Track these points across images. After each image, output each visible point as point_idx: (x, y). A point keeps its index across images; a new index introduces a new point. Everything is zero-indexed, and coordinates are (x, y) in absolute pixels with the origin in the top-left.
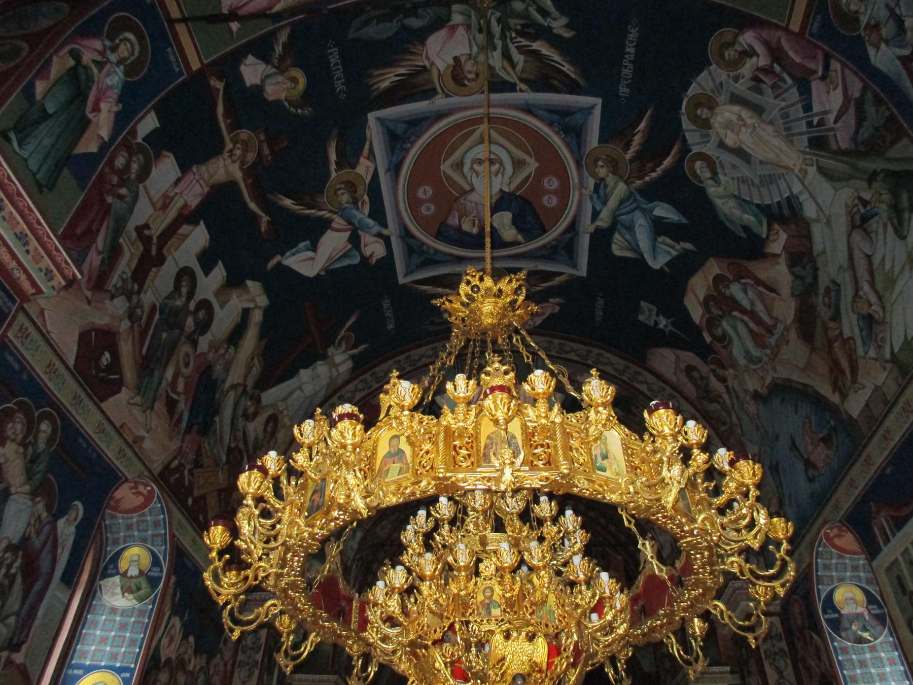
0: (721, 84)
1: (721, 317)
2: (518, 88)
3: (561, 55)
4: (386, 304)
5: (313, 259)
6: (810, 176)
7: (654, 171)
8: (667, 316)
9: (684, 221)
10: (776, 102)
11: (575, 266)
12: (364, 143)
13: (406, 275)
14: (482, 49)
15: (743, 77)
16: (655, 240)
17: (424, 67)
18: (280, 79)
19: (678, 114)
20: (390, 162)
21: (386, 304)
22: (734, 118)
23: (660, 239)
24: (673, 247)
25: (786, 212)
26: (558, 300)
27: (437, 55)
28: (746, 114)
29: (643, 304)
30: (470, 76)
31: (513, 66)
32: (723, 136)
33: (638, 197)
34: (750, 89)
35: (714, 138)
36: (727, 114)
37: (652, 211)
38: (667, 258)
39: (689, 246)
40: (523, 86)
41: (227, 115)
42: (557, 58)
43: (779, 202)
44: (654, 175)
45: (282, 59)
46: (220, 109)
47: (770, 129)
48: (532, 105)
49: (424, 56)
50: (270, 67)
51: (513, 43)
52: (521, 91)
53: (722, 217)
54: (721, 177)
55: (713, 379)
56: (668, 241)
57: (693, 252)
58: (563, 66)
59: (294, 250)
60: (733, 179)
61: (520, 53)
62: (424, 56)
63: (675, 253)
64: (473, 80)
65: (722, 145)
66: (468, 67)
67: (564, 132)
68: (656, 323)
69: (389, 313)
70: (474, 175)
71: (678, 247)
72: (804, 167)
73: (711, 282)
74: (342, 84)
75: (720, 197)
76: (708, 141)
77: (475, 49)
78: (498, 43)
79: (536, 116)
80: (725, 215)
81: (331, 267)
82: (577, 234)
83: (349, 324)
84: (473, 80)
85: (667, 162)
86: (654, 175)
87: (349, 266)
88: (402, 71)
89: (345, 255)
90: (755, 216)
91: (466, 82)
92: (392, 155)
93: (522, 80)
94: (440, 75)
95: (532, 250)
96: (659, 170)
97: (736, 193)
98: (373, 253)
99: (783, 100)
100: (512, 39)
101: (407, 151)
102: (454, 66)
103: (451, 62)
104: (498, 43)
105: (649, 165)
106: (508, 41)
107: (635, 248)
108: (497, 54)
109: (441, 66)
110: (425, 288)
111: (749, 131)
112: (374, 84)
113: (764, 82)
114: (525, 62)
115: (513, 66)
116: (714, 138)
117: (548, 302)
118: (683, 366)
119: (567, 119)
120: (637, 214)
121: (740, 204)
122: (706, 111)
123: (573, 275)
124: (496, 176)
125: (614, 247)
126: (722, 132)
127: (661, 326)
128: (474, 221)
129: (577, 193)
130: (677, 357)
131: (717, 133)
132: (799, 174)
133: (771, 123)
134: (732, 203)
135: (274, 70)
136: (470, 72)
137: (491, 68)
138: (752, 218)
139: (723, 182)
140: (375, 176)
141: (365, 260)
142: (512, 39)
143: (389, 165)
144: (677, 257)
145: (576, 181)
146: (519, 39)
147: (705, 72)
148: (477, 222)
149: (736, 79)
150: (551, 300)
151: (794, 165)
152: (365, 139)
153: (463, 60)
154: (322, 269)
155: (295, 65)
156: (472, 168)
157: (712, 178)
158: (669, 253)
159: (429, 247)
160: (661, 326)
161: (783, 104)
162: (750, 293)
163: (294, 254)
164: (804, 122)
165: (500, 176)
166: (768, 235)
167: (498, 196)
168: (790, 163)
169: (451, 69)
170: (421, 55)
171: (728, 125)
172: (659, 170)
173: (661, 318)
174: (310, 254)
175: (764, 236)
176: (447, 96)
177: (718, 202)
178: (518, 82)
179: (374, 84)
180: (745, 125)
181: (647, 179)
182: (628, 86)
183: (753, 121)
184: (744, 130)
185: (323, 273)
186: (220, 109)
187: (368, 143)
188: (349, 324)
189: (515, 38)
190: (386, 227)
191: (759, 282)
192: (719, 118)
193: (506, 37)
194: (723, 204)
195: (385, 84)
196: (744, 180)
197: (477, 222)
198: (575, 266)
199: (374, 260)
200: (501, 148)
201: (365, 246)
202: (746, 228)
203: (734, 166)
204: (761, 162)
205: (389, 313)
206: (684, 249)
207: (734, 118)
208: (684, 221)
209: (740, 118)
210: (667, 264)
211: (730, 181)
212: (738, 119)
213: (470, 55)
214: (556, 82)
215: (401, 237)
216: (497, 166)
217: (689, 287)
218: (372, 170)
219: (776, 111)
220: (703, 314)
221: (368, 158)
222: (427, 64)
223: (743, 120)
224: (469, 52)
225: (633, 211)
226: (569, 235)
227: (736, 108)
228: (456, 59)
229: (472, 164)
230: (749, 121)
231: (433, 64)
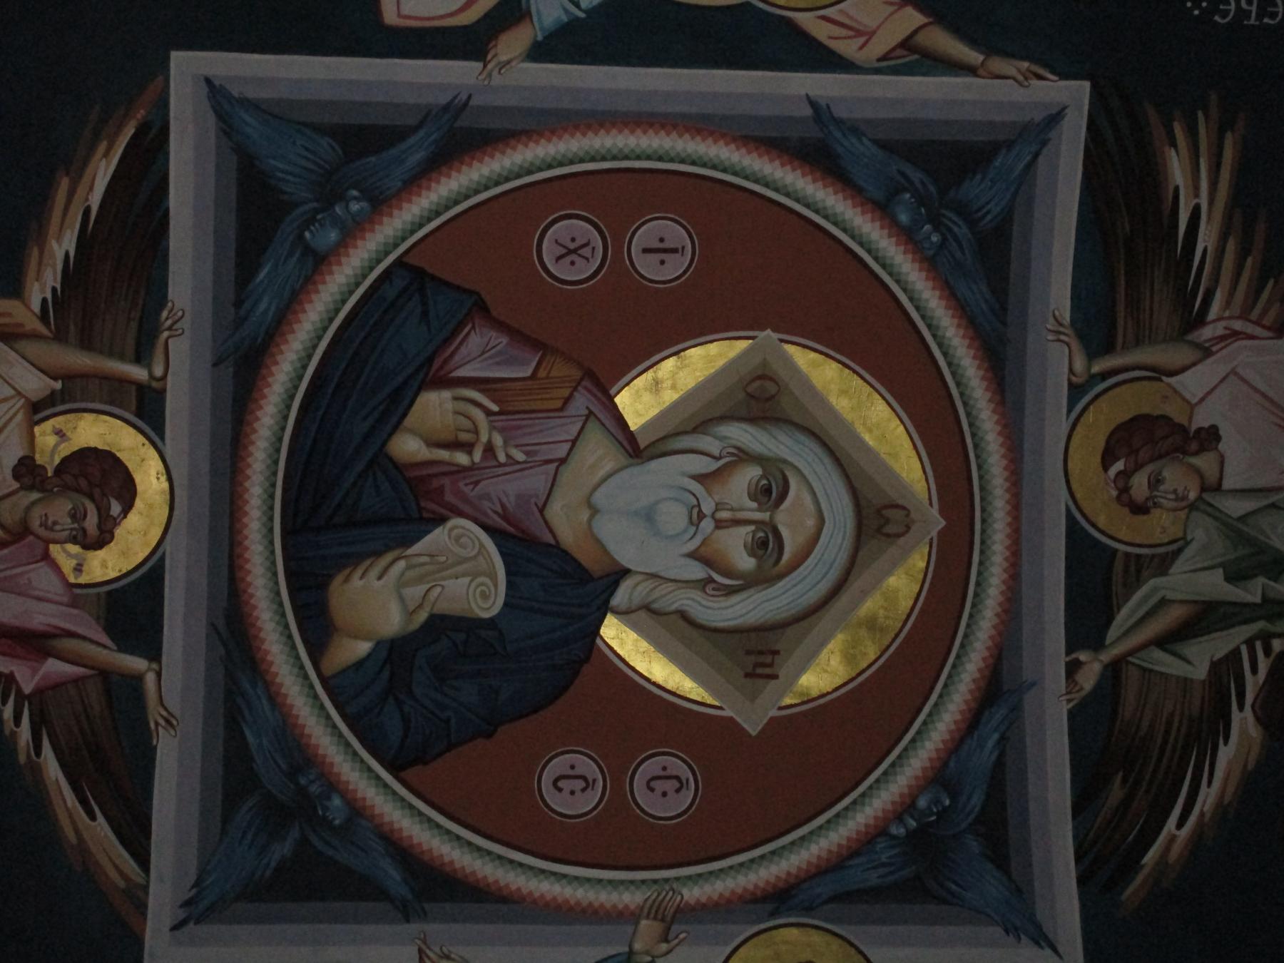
2: (1083, 656)
3: (1221, 808)
12: (973, 42)
13: (215, 91)
14: (1234, 530)
17: (1200, 321)
20: (854, 129)
27: (1233, 372)
30: (1139, 484)
31: (1165, 641)
40: (1088, 679)
42: (1208, 798)
48: (1016, 709)
49: (1238, 325)
51: (1250, 643)
52: (1073, 668)
58: (1180, 824)
61: (1215, 666)
62: (1238, 325)
64: (1124, 490)
66: (1176, 477)
67: (911, 835)
70: (702, 465)
74: (1242, 14)
77: (1235, 507)
78: (1251, 593)
79: (972, 723)
82: (406, 913)
84: (1124, 490)
88: (1206, 238)
91: (1119, 466)
92: (884, 145)
93: (1114, 670)
94: (1158, 373)
95: (275, 699)
100: (1266, 638)
101: (882, 208)
102: (1183, 430)
103: (1201, 420)
104: (1251, 593)
106: (1260, 625)
108: (1214, 585)
109: (1193, 383)
110: (102, 172)
112: (1192, 132)
114: (1185, 683)
115: (1165, 641)
119: (973, 844)
123: (141, 908)
124: (693, 555)
128: (468, 447)
129: (630, 899)
136: (1155, 482)
137: (1163, 564)
140: (826, 60)
142: (1266, 638)
143: (839, 122)
145: (692, 894)
146: (1263, 665)
148: (462, 458)
152: (991, 50)
153: (1204, 462)
156: (743, 456)
159: (352, 231)
165: (697, 571)
167: (586, 557)
169: (1180, 418)
170: (1244, 316)
176: (1076, 391)
178: (1106, 657)
179: (1192, 132)
187: (973, 56)
189: (1267, 651)
190: (541, 52)
193: (1270, 618)
195: (1176, 169)
197: (462, 458)
200: (823, 588)
213: (1218, 488)
214: (1116, 792)
215: (455, 108)
216: (746, 563)
218: (848, 48)
221: (907, 44)
222: (1207, 333)
224: (1228, 484)
226: (392, 875)
228: (1210, 437)
229: (759, 459)
231: (1207, 353)
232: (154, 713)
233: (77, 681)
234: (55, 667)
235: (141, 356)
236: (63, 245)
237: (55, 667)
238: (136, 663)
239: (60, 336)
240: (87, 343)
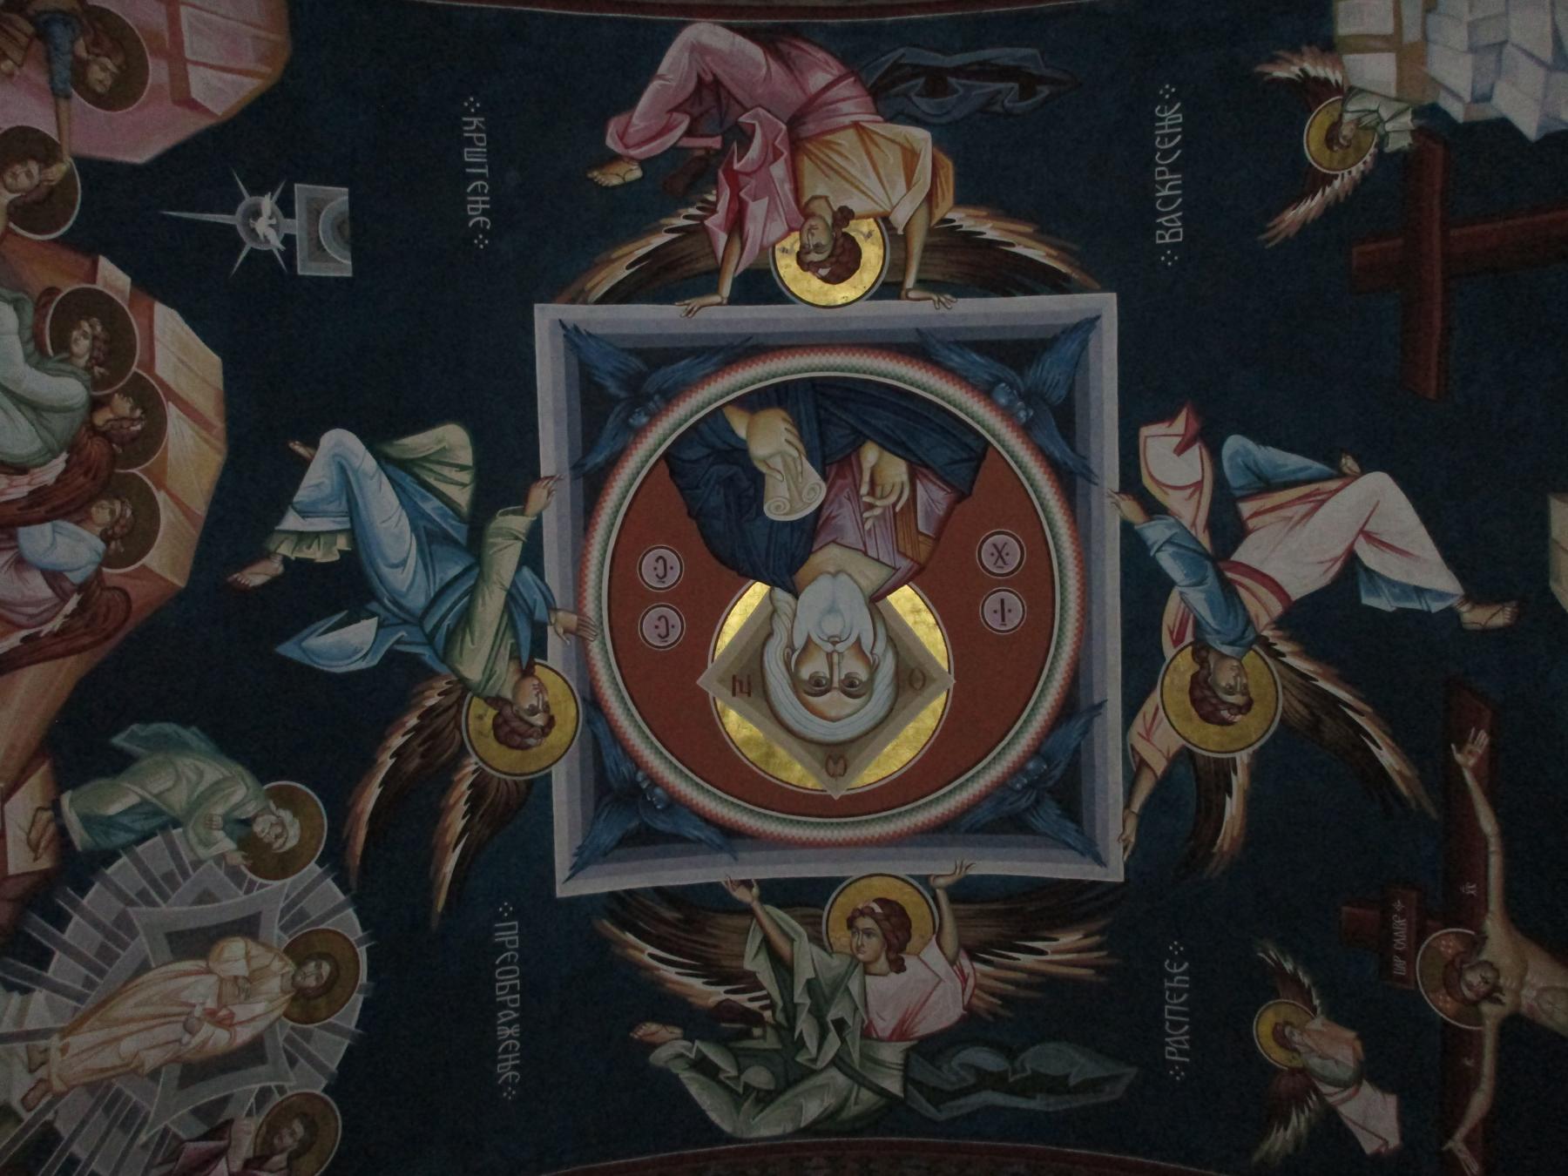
0: (292, 1062)
1: (96, 404)
2: (755, 890)
3: (661, 981)
4: (1170, 228)
5: (1370, 537)
6: (19, 1070)
7: (398, 754)
8: (261, 258)
9: (288, 649)
10: (161, 1126)
11: (573, 337)
12: (1146, 806)
13: (1090, 323)
14: (839, 984)
15: (249, 1114)
16: (352, 534)
17: (973, 957)
18: (1314, 1062)
19: (371, 937)
20: (1086, 731)
21: (1170, 228)
22: (241, 1012)
23: (342, 543)
24: (302, 537)
25: (37, 927)
26: (612, 178)
27: (941, 980)
28: (219, 1039)
29: (340, 265)
30: (866, 923)
31: (767, 942)
32: (255, 950)
33: (426, 653)
34: (225, 1100)
35: (273, 931)
36: (259, 1008)
37: (380, 626)
38: (302, 495)
39: (256, 576)
40: (742, 895)
41: (1468, 1083)
42: (669, 973)
43: (61, 920)
44: (397, 741)
45: (1298, 1100)
46: (1479, 1103)
47: (152, 1059)
48: (720, 849)
49: (971, 982)
50: (1330, 1100)
51: (768, 996)
52: (747, 884)
53: (190, 735)
54: (226, 844)
55: (41, 119)
56: (317, 554)
57: (242, 567)
58: (652, 956)
59: (1414, 605)
60: (197, 864)
61: (752, 975)
62: (971, 982)
63: (291, 522)
64: (862, 913)
65: (248, 927)
66: (872, 945)
67: (637, 786)
68: (286, 206)
69: (1168, 185)
70: (867, 643)
71: (285, 549)
72: (41, 1073)
73: (161, 497)
74: (1171, 977)
75: (216, 787)
76: (284, 912)
77: (854, 986)
78: (801, 996)
79: (708, 820)
80: (183, 747)
81: (1317, 467)
82: (576, 467)
83: (1310, 207)
84: (862, 913)
85: (372, 794)
86: (397, 741)
87: (1263, 439)
88: (1026, 960)
89: (1266, 484)
90: (110, 823)
91: (878, 909)
92: (1077, 751)
93: (748, 911)
94: (938, 932)
95: (706, 378)
96: (386, 761)
97: (176, 832)
98: (1181, 450)
99: (145, 1146)
100: (772, 1006)
101: (1036, 752)
102: (902, 948)
103: (910, 962)
104: (801, 996)
105: (415, 762)
106: (780, 1004)
107: (402, 471)
108: (804, 972)
109: (932, 954)
110: (1037, 253)
111: (198, 1012)
113: (205, 1137)
114: (741, 956)
115: (767, 942)
116: (273, 931)
117: (643, 163)
118: (158, 72)
119: (634, 824)
120: (417, 601)
121: (157, 812)
122: (311, 982)
124: (809, 641)
125: (466, 456)
126: (262, 957)
127: (267, 203)
128: (872, 493)
129: (590, 608)
130: (193, 105)
131: (267, 947)
132: (42, 1043)
133: (155, 1075)
134: (178, 800)
135: (1326, 1089)
136: (868, 933)
137: (816, 939)
138: (114, 809)
139: (220, 834)
140: (1130, 711)
141: (1209, 437)
142: (772, 1006)
143: (1089, 724)
144: (281, 516)
145: (594, 647)
146: (755, 1005)
147: (333, 1066)
148: (864, 489)
149: (264, 1095)
150: (636, 173)
151: (64, 1050)
152: (1141, 817)
153: (882, 964)
154: (1346, 478)
155: (1269, 1070)
156: (873, 669)
157: (248, 823)
158: (304, 514)
159: (1007, 413)
160: (267, 203)
161: (143, 1138)
162: (39, 587)
163: (1420, 591)
164: (83, 1156)
165: (799, 642)
166: (56, 806)
167: (804, 572)
168: (78, 1041)
169: (909, 947)
170: (977, 986)
171: (246, 986)
172: (386, 761)
173: (276, 243)
174: (1370, 557)
175: (66, 799)
176: (924, 880)
177: (213, 770)
178: (756, 906)
180: (211, 1014)
181: (413, 721)
182: (501, 948)
183: (197, 1040)
184: (211, 1004)
185: (1349, 463)
186: (1479, 1103)
187: (1136, 806)
188: (1310, 207)
189: (764, 1008)
190: (1127, 528)
191: (33, 651)
192: (274, 985)
193: (784, 1009)
194: (201, 774)
195: (1069, 939)
196: (165, 885)
197: (864, 489)
198: (573, 337)
199: (1180, 425)
201: (1198, 485)
202: (120, 763)
203: (205, 897)
204: (144, 967)
205: (1168, 185)
206: (267, 555)
207: (241, 1012)
208: (288, 649)
209: (227, 1023)
210: (303, 464)
211: (202, 852)
212: (232, 1015)
213: (866, 972)
214: (670, 915)
215: (1088, 475)
216: (805, 673)
217: (221, 445)
218: (1138, 725)
219: (153, 1110)
220: (149, 364)
221: (1143, 763)
222: (965, 962)
223: (220, 1023)
224: (869, 979)
225: (433, 602)
226: (599, 458)
227: (244, 1035)
228: (898, 966)
229: (872, 679)
230: (207, 1030)
231: (952, 963)
232: (695, 302)
233: (714, 253)
234: (722, 239)
235: (921, 283)
236: (990, 230)
237: (722, 239)
238: (726, 289)
239: (931, 231)
240: (927, 248)
